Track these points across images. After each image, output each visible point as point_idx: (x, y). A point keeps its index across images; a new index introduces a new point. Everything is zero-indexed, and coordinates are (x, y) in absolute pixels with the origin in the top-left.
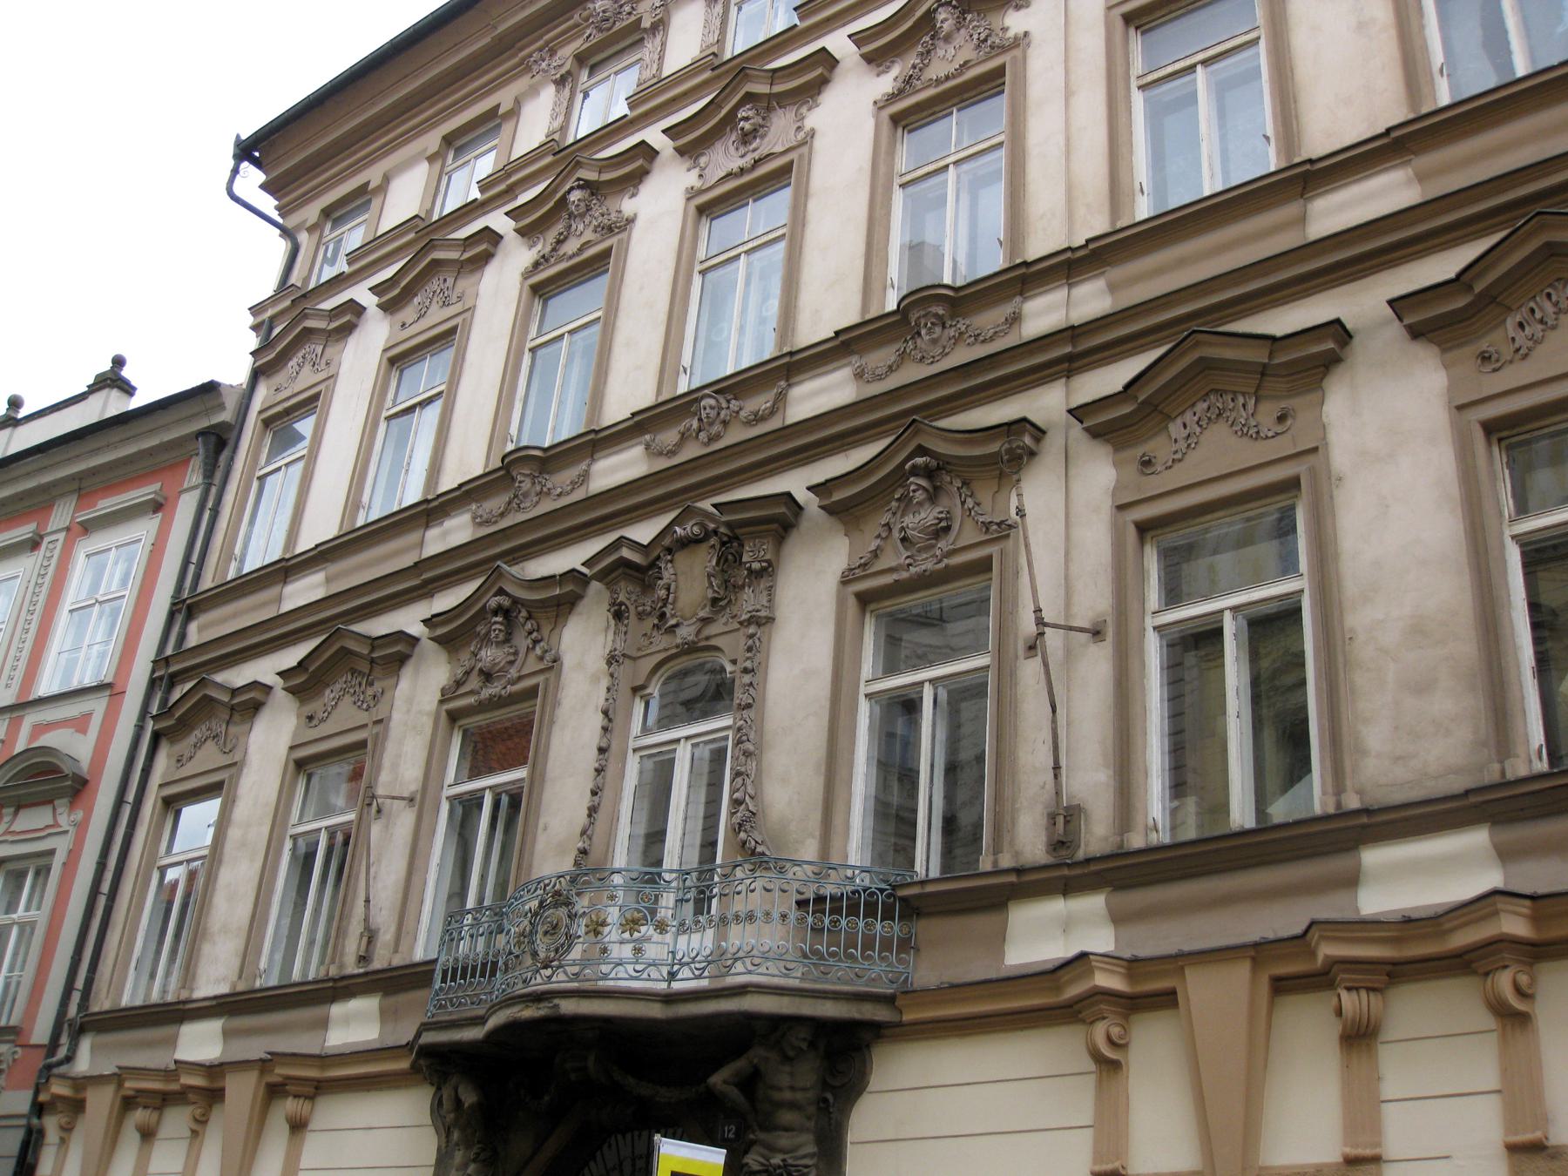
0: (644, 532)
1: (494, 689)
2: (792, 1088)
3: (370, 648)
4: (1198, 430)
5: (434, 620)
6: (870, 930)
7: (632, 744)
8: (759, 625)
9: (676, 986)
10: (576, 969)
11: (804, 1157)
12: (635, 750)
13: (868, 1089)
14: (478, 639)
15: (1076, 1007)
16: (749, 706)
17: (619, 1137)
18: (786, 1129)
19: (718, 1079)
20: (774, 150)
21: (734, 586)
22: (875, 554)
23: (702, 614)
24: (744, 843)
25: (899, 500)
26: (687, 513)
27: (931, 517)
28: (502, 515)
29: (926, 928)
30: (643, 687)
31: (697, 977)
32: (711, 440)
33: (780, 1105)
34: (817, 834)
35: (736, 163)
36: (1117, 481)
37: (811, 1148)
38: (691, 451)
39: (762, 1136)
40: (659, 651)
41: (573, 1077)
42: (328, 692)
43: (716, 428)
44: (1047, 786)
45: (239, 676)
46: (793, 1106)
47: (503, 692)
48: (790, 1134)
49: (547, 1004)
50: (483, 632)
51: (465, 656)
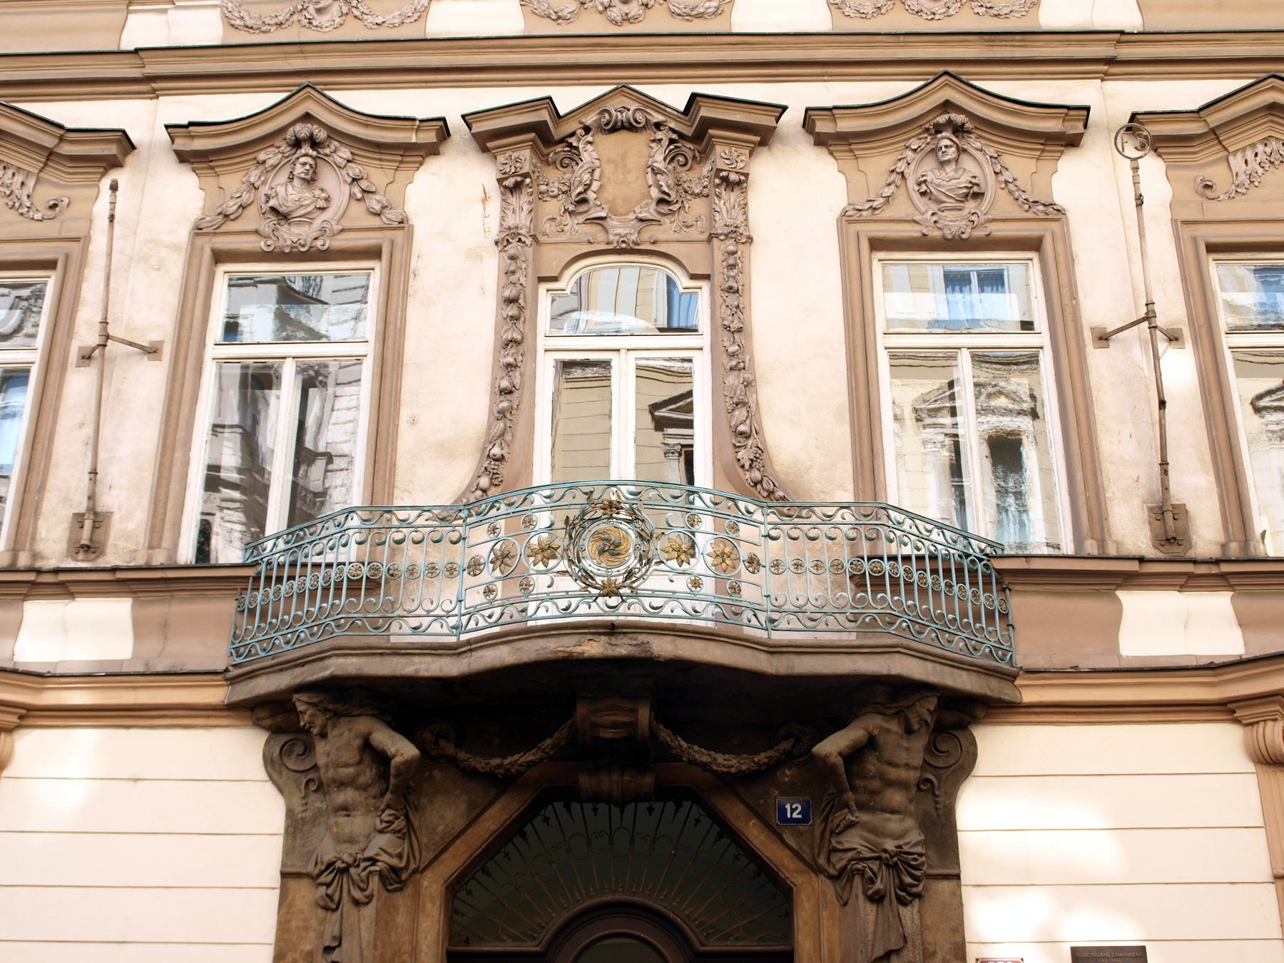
1: (291, 235)
2: (907, 766)
3: (57, 141)
4: (1260, 171)
5: (191, 128)
6: (976, 600)
7: (542, 343)
9: (777, 636)
10: (657, 602)
11: (916, 844)
13: (973, 773)
14: (261, 168)
15: (1230, 706)
16: (740, 330)
17: (559, 806)
18: (893, 812)
19: (833, 746)
21: (686, 192)
23: (644, 215)
26: (623, 90)
29: (1023, 605)
31: (808, 630)
32: (627, 19)
33: (890, 783)
34: (851, 487)
36: (1173, 196)
37: (915, 836)
39: (864, 817)
41: (608, 734)
44: (1142, 481)
46: (902, 785)
47: (319, 244)
48: (896, 817)
49: (626, 640)
50: (271, 162)
51: (233, 181)
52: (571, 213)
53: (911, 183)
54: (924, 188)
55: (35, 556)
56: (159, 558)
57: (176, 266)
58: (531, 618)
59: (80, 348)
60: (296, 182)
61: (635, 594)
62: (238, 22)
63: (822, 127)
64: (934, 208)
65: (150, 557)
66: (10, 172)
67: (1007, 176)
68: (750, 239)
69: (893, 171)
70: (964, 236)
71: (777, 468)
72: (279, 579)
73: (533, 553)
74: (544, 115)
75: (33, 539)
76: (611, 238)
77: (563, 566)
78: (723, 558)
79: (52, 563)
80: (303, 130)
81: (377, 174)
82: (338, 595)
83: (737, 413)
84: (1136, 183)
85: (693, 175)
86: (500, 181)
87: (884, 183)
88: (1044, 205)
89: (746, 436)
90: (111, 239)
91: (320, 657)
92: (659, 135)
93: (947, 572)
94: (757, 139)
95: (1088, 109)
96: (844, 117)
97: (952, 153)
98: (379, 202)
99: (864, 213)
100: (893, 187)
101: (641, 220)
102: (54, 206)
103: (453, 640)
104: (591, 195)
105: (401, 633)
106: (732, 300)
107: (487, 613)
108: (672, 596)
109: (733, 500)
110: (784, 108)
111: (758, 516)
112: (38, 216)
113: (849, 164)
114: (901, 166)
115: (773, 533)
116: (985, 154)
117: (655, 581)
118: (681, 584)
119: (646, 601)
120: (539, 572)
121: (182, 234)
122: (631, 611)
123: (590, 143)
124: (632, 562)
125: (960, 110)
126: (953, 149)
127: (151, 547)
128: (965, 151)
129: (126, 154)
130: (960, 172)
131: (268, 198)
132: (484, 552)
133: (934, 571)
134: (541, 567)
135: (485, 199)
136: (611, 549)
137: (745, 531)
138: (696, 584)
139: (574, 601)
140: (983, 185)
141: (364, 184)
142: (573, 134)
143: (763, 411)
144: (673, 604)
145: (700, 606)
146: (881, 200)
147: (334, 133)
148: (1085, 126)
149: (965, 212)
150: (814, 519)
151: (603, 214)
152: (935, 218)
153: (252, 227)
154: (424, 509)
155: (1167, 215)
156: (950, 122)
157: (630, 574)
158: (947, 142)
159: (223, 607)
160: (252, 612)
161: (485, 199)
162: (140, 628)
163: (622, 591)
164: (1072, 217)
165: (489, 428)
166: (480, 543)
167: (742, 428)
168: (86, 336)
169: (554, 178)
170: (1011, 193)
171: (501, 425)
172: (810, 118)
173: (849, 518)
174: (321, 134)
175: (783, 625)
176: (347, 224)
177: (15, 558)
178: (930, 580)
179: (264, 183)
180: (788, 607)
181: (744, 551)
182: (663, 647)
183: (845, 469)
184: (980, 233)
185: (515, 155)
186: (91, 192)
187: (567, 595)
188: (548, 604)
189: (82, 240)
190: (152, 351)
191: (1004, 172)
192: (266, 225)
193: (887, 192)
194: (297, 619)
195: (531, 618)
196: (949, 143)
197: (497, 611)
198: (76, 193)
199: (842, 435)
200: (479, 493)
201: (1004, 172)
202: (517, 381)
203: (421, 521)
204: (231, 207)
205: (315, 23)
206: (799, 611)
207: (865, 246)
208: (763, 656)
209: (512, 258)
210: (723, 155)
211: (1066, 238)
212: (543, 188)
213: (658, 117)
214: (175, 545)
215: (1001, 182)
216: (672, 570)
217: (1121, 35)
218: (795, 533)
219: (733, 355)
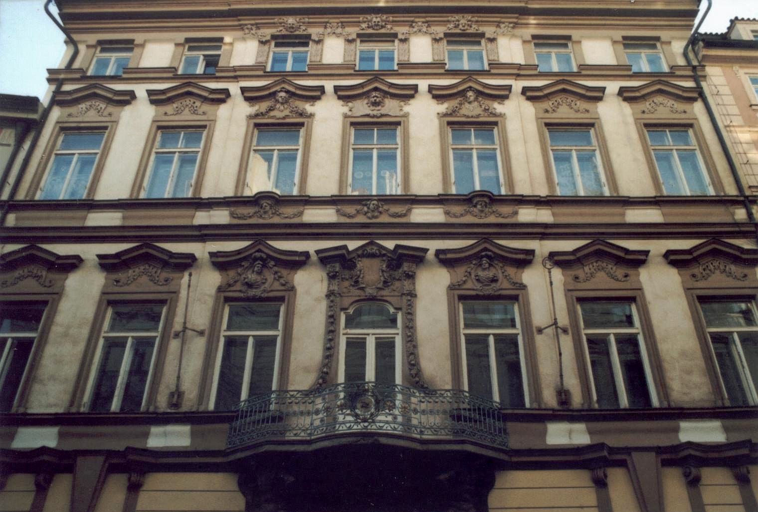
0: (353, 245)
1: (252, 293)
7: (342, 331)
8: (411, 297)
9: (425, 437)
10: (381, 424)
12: (344, 334)
16: (412, 328)
20: (390, 114)
22: (465, 282)
24: (417, 382)
25: (474, 264)
27: (491, 274)
28: (250, 217)
30: (346, 309)
31: (434, 435)
32: (374, 217)
35: (368, 111)
38: (361, 219)
40: (356, 296)
42: (131, 271)
43: (376, 214)
45: (63, 249)
47: (263, 295)
50: (246, 266)
51: (232, 273)
52: (353, 286)
53: (473, 276)
54: (477, 278)
55: (156, 407)
56: (202, 409)
57: (210, 302)
58: (337, 430)
59: (175, 332)
60: (255, 273)
61: (374, 422)
62: (235, 216)
63: (442, 256)
65: (198, 408)
66: (151, 268)
67: (506, 273)
68: (416, 296)
69: (466, 272)
71: (425, 377)
72: (246, 416)
73: (338, 407)
74: (344, 252)
75: (155, 402)
76: (367, 294)
77: (348, 412)
78: (405, 411)
79: (161, 410)
80: (258, 255)
81: (284, 272)
82: (268, 422)
83: (411, 357)
84: (550, 277)
85: (396, 273)
86: (328, 274)
89: (413, 365)
90: (188, 293)
91: (261, 445)
92: (384, 258)
93: (484, 415)
97: (487, 265)
98: (284, 280)
101: (378, 288)
102: (166, 281)
103: (308, 438)
104: (360, 279)
105: (290, 436)
106: (409, 317)
107: (321, 429)
108: (387, 422)
109: (408, 388)
111: (417, 394)
112: (160, 284)
113: (451, 271)
114: (469, 270)
115: (423, 400)
117: (381, 418)
118: (390, 418)
119: (378, 424)
120: (340, 414)
121: (213, 291)
122: (373, 428)
123: (361, 261)
124: (373, 410)
127: (198, 405)
129: (193, 262)
131: (245, 278)
132: (320, 406)
133: (479, 414)
134: (340, 412)
135: (322, 281)
136: (366, 406)
137: (413, 400)
138: (395, 418)
139: (352, 424)
141: (279, 274)
142: (354, 258)
143: (420, 357)
144: (386, 425)
145: (396, 426)
146: (462, 282)
147: (269, 256)
148: (534, 257)
150: (437, 395)
151: (364, 286)
153: (239, 289)
154: (299, 391)
155: (562, 288)
157: (372, 414)
158: (484, 262)
159: (226, 426)
160: (235, 429)
161: (322, 281)
162: (193, 434)
163: (369, 421)
164: (529, 288)
165: (323, 360)
166: (319, 404)
167: (413, 362)
168: (177, 326)
169: (346, 274)
170: (508, 280)
171: (327, 360)
172: (438, 252)
173: (449, 394)
174: (265, 256)
175: (426, 433)
176: (273, 288)
177: (148, 409)
178: (478, 417)
179: (243, 273)
180: (428, 426)
181: (413, 406)
182: (384, 441)
183: (448, 378)
184: (497, 293)
185: (333, 265)
186: (180, 275)
187: (350, 422)
188: (343, 425)
189: (176, 293)
190: (201, 333)
192: (244, 288)
193: (464, 279)
194: (253, 431)
195: (337, 430)
197: (325, 428)
198: (176, 275)
199: (448, 365)
200: (318, 385)
202: (333, 345)
203: (298, 395)
204: (231, 282)
205: (263, 216)
206: (431, 428)
207: (456, 298)
208: (419, 444)
209: (332, 301)
210: (406, 267)
211: (527, 296)
212: (343, 276)
213: (384, 252)
214: (208, 404)
216: (387, 413)
217: (546, 226)
218: (430, 400)
219: (410, 336)
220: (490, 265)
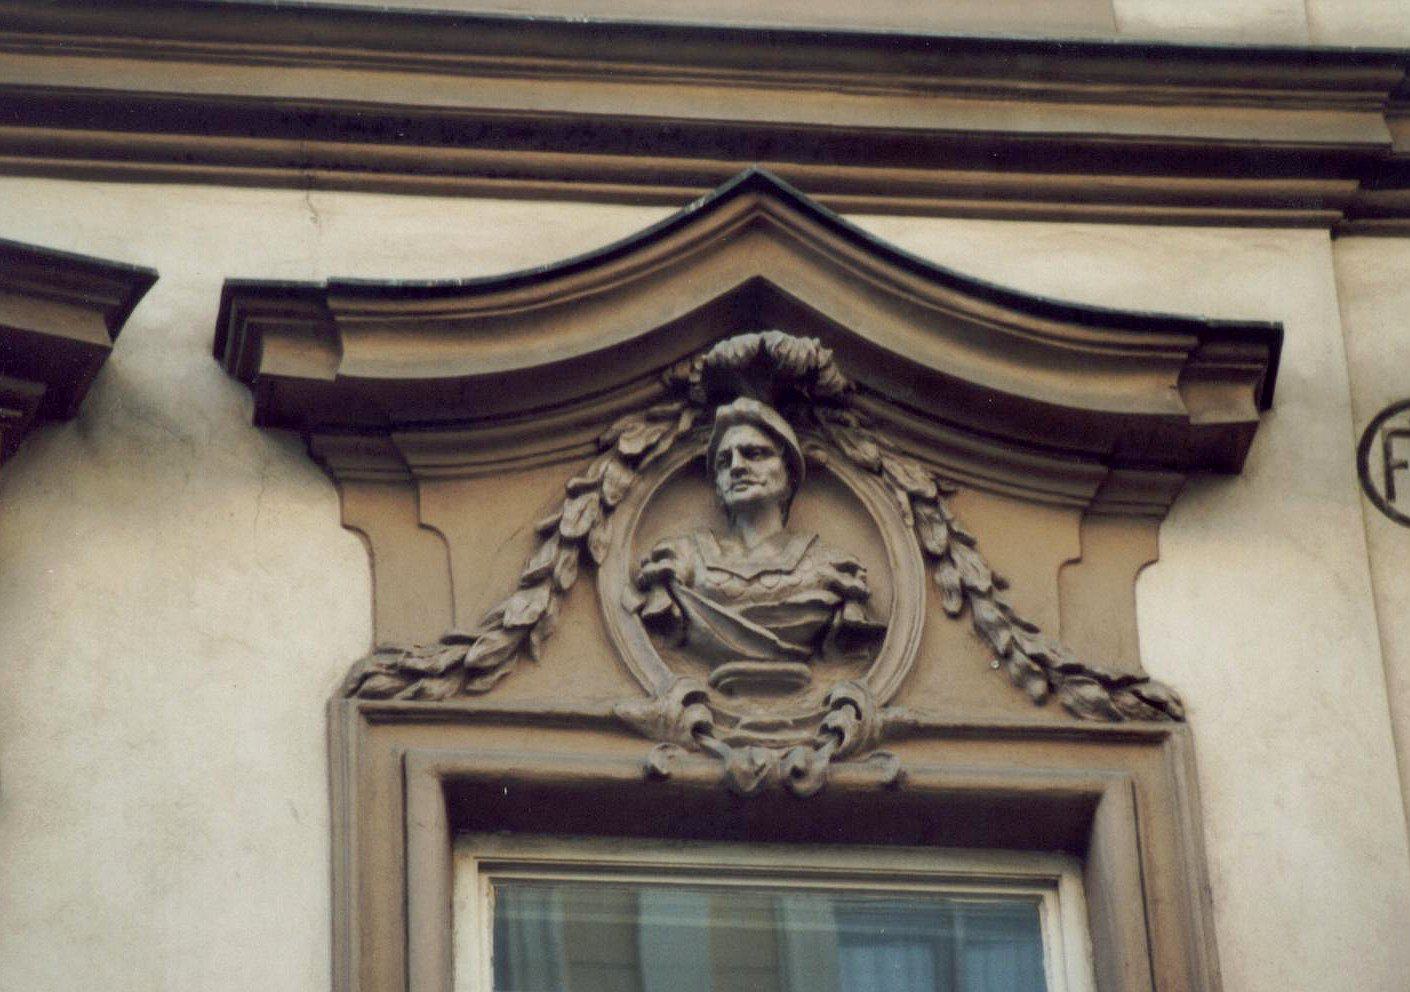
22: (524, 642)
25: (631, 462)
54: (660, 602)
63: (282, 360)
64: (696, 679)
67: (969, 567)
69: (547, 533)
70: (803, 786)
87: (516, 577)
88: (1106, 683)
94: (35, 390)
95: (1268, 338)
96: (366, 328)
97: (768, 475)
99: (435, 687)
100: (543, 593)
110: (139, 281)
113: (385, 513)
114: (575, 518)
116: (893, 486)
125: (802, 319)
126: (774, 463)
128: (818, 471)
130: (798, 546)
140: (880, 600)
146: (500, 640)
148: (1265, 400)
149: (808, 703)
152: (698, 714)
156: (762, 358)
158: (746, 436)
170: (982, 632)
184: (863, 773)
191: (960, 553)
193: (522, 608)
196: (757, 439)
201: (960, 553)
207: (429, 809)
215: (949, 592)
220: (803, 475)
